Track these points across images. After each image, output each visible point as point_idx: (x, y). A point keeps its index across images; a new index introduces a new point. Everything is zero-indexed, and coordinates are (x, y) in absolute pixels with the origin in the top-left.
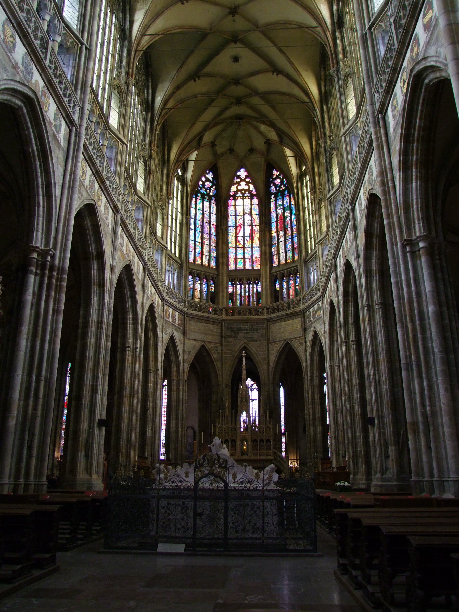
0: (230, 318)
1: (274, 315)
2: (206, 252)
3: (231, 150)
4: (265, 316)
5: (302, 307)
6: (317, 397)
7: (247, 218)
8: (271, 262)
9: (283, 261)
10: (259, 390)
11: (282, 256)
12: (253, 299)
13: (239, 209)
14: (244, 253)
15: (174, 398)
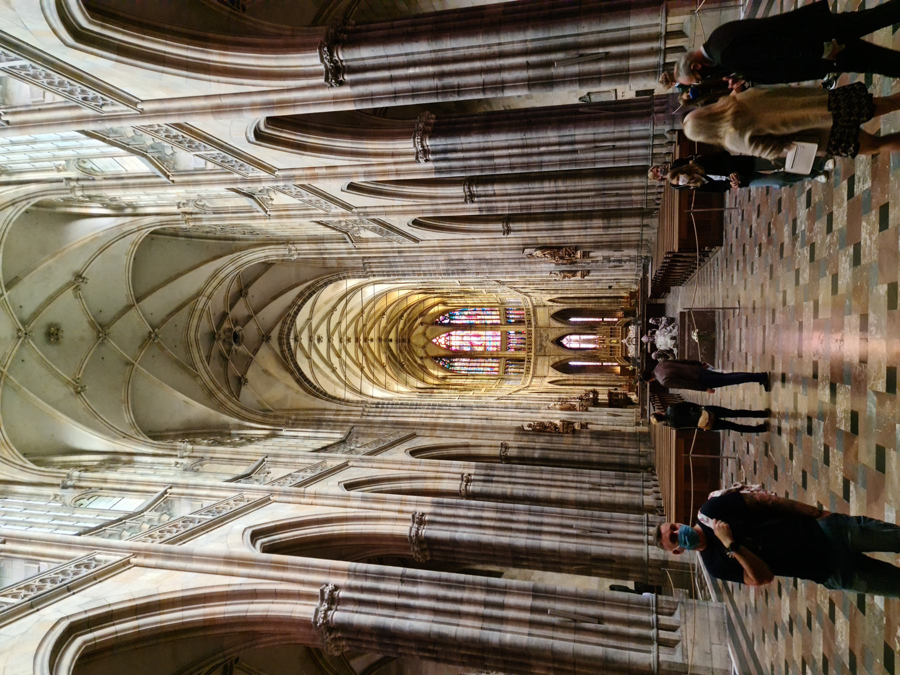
0: (533, 350)
1: (533, 324)
2: (490, 365)
3: (424, 347)
4: (533, 329)
5: (531, 307)
6: (585, 301)
7: (465, 338)
8: (497, 324)
9: (498, 317)
10: (571, 334)
11: (494, 317)
12: (519, 336)
13: (458, 343)
14: (490, 340)
15: (584, 383)
